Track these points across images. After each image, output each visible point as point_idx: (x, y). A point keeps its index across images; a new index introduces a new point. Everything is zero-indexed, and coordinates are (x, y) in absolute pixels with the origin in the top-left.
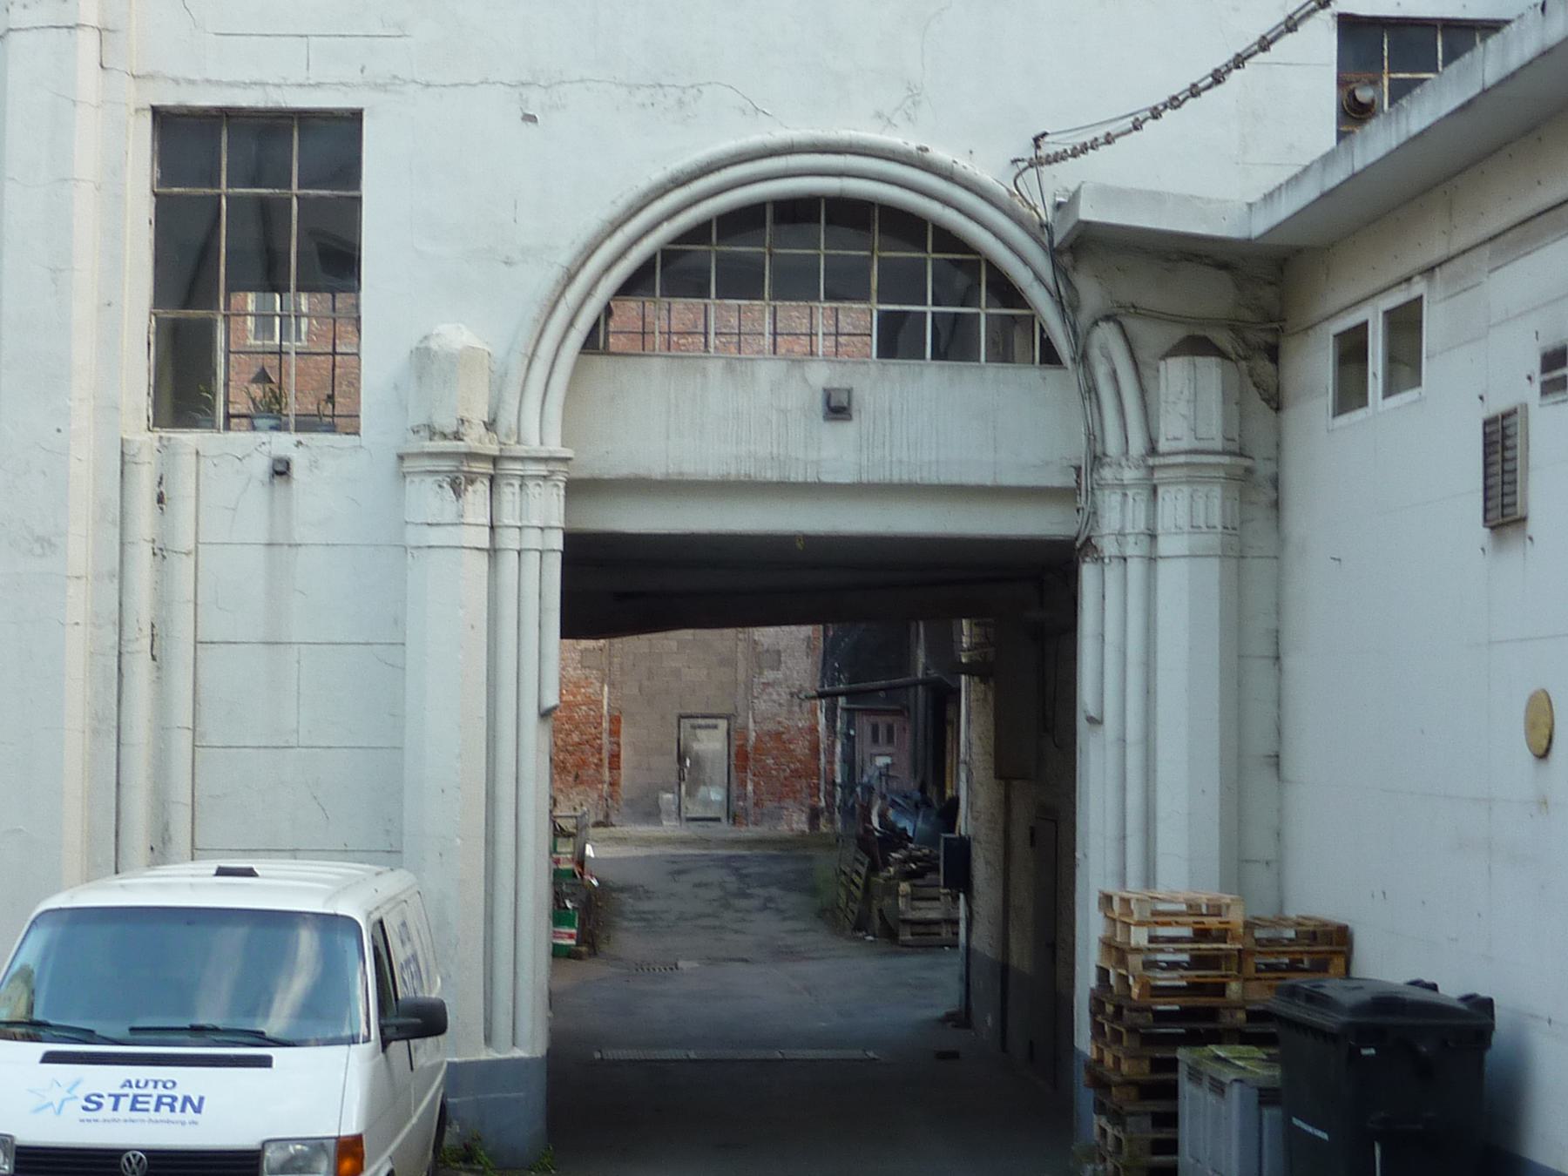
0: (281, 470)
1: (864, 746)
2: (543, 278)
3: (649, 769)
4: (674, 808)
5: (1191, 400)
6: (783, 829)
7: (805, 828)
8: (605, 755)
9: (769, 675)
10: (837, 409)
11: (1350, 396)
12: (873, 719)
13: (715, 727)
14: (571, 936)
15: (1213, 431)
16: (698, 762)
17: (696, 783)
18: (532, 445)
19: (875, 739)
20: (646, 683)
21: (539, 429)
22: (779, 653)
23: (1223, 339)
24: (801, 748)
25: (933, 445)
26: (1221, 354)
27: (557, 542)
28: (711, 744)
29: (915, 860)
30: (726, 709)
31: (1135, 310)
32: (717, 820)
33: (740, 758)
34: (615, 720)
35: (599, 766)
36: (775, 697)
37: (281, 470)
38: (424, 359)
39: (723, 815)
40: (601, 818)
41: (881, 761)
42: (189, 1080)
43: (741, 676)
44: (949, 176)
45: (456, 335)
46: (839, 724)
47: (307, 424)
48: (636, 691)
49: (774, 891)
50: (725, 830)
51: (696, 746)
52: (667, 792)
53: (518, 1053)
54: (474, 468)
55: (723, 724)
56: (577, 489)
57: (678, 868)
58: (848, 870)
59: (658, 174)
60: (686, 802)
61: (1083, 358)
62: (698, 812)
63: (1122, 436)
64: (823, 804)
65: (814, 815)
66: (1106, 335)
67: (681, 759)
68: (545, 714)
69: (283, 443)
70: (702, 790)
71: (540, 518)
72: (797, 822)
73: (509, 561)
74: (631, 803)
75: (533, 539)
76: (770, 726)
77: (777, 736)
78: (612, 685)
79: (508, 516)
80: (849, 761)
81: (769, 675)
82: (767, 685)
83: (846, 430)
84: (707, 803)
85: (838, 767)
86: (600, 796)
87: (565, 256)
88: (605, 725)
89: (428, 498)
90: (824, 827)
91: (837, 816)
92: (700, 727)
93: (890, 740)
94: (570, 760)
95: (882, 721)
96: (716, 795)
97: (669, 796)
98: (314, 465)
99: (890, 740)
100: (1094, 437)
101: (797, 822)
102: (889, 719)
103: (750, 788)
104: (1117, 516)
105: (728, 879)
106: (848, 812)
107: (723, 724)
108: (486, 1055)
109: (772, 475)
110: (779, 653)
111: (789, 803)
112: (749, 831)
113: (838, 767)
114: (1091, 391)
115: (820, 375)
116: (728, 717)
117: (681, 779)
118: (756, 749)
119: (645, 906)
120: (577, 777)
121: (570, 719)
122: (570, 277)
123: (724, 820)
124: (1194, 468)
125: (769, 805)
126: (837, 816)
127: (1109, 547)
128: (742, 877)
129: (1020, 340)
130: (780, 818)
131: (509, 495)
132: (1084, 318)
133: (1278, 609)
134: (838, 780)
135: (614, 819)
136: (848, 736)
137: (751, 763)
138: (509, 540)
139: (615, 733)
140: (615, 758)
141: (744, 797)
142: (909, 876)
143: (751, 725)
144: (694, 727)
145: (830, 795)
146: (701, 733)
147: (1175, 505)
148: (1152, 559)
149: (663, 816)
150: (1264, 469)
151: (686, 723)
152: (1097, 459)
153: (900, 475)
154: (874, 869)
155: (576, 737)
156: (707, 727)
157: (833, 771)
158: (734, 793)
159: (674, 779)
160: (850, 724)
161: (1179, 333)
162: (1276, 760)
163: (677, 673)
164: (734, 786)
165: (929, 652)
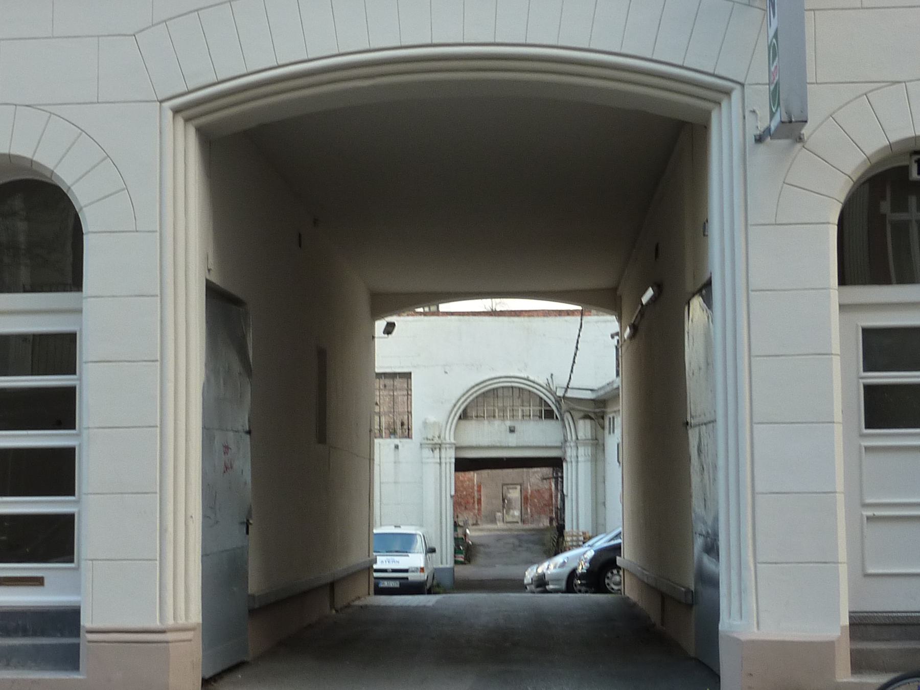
0: (397, 447)
2: (449, 406)
5: (584, 428)
6: (541, 525)
10: (512, 430)
11: (610, 433)
15: (589, 436)
16: (509, 501)
18: (448, 441)
21: (449, 438)
23: (593, 416)
24: (547, 496)
25: (536, 436)
26: (591, 418)
27: (453, 460)
30: (521, 481)
31: (573, 409)
33: (525, 499)
34: (479, 487)
37: (397, 447)
38: (425, 424)
42: (396, 558)
44: (534, 382)
45: (432, 419)
47: (403, 437)
49: (530, 545)
50: (520, 525)
51: (509, 495)
53: (448, 566)
54: (437, 447)
55: (519, 487)
56: (458, 448)
57: (499, 539)
59: (473, 384)
61: (563, 420)
62: (509, 519)
63: (571, 436)
65: (551, 520)
66: (567, 415)
67: (503, 500)
68: (451, 497)
69: (397, 441)
70: (511, 512)
71: (450, 456)
72: (546, 523)
73: (443, 465)
75: (448, 460)
76: (535, 488)
79: (443, 456)
83: (514, 435)
84: (513, 516)
87: (454, 402)
88: (476, 488)
89: (427, 453)
96: (517, 513)
98: (403, 446)
100: (565, 436)
104: (570, 453)
108: (441, 566)
109: (498, 444)
112: (527, 526)
114: (564, 426)
115: (508, 423)
117: (503, 507)
119: (487, 550)
122: (455, 405)
124: (585, 445)
125: (536, 516)
127: (568, 459)
128: (520, 541)
129: (549, 415)
131: (443, 451)
132: (562, 411)
133: (604, 471)
138: (443, 461)
139: (479, 491)
145: (556, 513)
146: (511, 491)
147: (581, 450)
148: (577, 462)
150: (601, 442)
151: (505, 487)
152: (566, 441)
153: (525, 444)
161: (582, 414)
162: (604, 504)
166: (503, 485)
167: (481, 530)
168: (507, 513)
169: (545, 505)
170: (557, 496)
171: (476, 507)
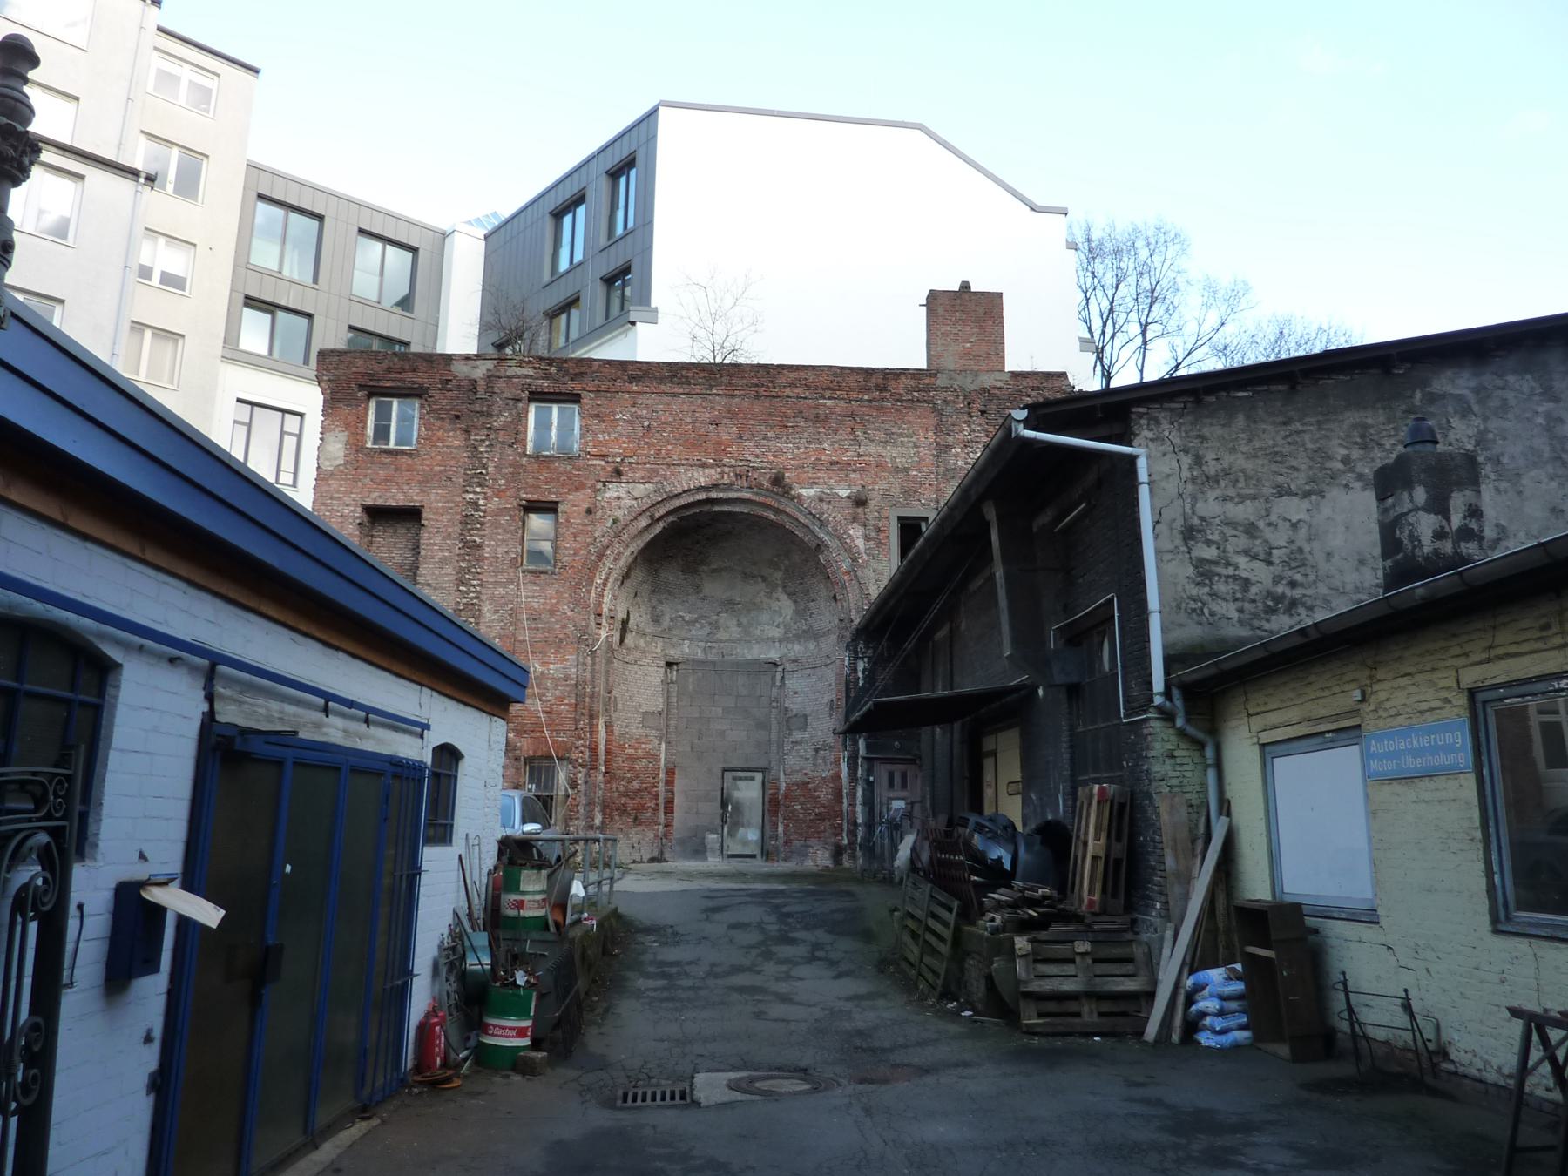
1: (881, 791)
4: (717, 846)
6: (809, 865)
7: (829, 863)
8: (661, 801)
9: (797, 735)
12: (890, 767)
13: (753, 779)
14: (521, 1033)
16: (738, 808)
17: (736, 825)
19: (891, 785)
22: (805, 716)
24: (825, 794)
28: (749, 792)
29: (1032, 903)
30: (762, 764)
32: (753, 856)
33: (773, 804)
34: (670, 772)
35: (655, 810)
39: (757, 851)
40: (655, 854)
41: (898, 804)
43: (774, 736)
49: (821, 935)
50: (760, 865)
51: (737, 794)
55: (759, 776)
57: (714, 905)
58: (918, 913)
60: (728, 841)
62: (736, 849)
64: (845, 842)
65: (838, 853)
67: (724, 805)
70: (741, 831)
74: (682, 842)
76: (797, 777)
78: (668, 743)
80: (869, 802)
81: (797, 735)
84: (745, 843)
85: (859, 809)
86: (656, 836)
88: (662, 776)
90: (846, 863)
91: (859, 853)
94: (631, 804)
95: (898, 769)
96: (753, 835)
99: (904, 786)
101: (820, 858)
103: (780, 829)
105: (767, 919)
106: (869, 849)
107: (759, 776)
110: (805, 716)
111: (813, 842)
112: (781, 867)
113: (859, 809)
116: (763, 770)
117: (724, 822)
118: (786, 797)
119: (672, 954)
120: (636, 818)
121: (631, 769)
126: (859, 853)
128: (784, 917)
130: (806, 855)
135: (667, 856)
136: (870, 784)
137: (782, 809)
139: (669, 782)
140: (669, 805)
141: (775, 837)
142: (1025, 926)
143: (782, 777)
144: (735, 778)
145: (852, 834)
146: (741, 784)
151: (728, 775)
154: (970, 912)
155: (636, 785)
156: (746, 778)
157: (854, 813)
158: (767, 835)
159: (718, 821)
160: (869, 771)
163: (722, 733)
164: (767, 827)
165: (1016, 641)
167: (667, 874)
168: (731, 834)
169: (821, 817)
170: (853, 794)
171: (661, 817)
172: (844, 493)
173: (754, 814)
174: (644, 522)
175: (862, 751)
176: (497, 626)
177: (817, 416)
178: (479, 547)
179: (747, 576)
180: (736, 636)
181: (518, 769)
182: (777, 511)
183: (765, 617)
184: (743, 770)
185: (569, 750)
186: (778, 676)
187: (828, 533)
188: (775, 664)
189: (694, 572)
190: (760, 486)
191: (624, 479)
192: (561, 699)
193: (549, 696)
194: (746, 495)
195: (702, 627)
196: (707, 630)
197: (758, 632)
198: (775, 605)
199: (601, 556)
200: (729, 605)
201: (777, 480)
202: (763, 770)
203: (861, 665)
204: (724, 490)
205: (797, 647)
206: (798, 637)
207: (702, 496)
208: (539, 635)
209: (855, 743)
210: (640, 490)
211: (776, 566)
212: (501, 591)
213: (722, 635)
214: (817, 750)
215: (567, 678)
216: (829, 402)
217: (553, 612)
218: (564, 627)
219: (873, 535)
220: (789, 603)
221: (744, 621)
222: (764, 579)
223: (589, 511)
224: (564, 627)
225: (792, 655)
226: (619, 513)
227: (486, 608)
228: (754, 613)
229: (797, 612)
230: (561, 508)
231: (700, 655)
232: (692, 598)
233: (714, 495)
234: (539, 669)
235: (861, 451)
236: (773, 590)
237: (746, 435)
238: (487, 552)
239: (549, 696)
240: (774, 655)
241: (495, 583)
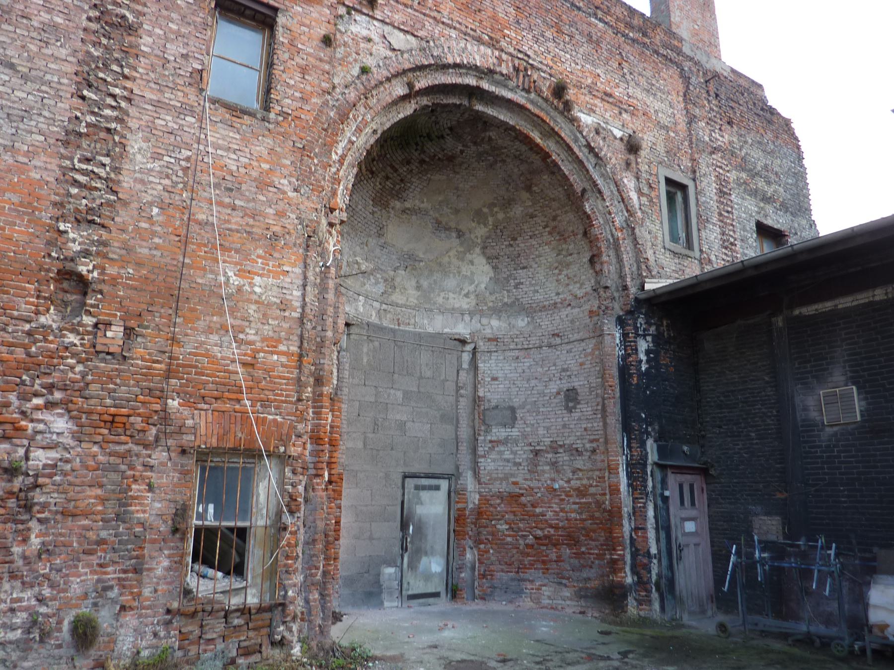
3: (371, 538)
4: (395, 584)
9: (498, 433)
12: (681, 478)
13: (437, 488)
17: (419, 553)
20: (370, 435)
22: (513, 410)
28: (433, 507)
30: (448, 468)
32: (436, 595)
33: (461, 523)
36: (507, 455)
39: (441, 589)
43: (465, 432)
46: (650, 484)
48: (360, 445)
51: (420, 510)
52: (390, 565)
55: (444, 484)
60: (409, 577)
62: (417, 586)
67: (404, 526)
70: (424, 560)
74: (350, 582)
77: (513, 498)
81: (498, 433)
82: (495, 443)
92: (424, 488)
93: (693, 503)
95: (687, 479)
96: (436, 565)
97: (391, 570)
99: (693, 503)
102: (689, 477)
107: (444, 484)
110: (513, 410)
111: (531, 574)
113: (651, 534)
116: (448, 477)
117: (404, 549)
123: (443, 595)
125: (503, 577)
130: (519, 593)
134: (654, 550)
144: (417, 488)
146: (425, 495)
149: (385, 596)
151: (410, 483)
159: (397, 549)
163: (402, 425)
166: (405, 477)
168: (412, 566)
170: (638, 513)
172: (618, 134)
173: (438, 536)
174: (400, 90)
175: (652, 456)
176: (157, 187)
177: (589, 35)
178: (131, 29)
179: (440, 226)
180: (413, 301)
181: (185, 473)
182: (552, 134)
183: (451, 282)
184: (427, 476)
185: (285, 441)
186: (466, 357)
187: (602, 175)
188: (463, 342)
189: (385, 206)
190: (539, 93)
191: (378, 14)
192: (272, 343)
193: (251, 334)
194: (519, 97)
195: (377, 283)
196: (381, 288)
197: (440, 300)
198: (466, 270)
199: (343, 118)
200: (410, 261)
201: (559, 90)
202: (448, 477)
203: (643, 345)
204: (497, 83)
205: (495, 323)
206: (496, 311)
207: (472, 81)
208: (236, 220)
209: (643, 444)
210: (399, 40)
211: (479, 217)
212: (167, 120)
213: (397, 297)
214: (537, 453)
215: (284, 306)
216: (601, 25)
217: (263, 184)
218: (281, 214)
219: (646, 190)
220: (487, 268)
221: (425, 284)
222: (460, 234)
223: (327, 41)
224: (281, 214)
225: (488, 332)
226: (370, 62)
227: (136, 144)
228: (437, 276)
229: (495, 280)
230: (281, 20)
231: (374, 319)
232: (373, 242)
233: (485, 85)
234: (235, 281)
235: (630, 91)
236: (469, 250)
237: (524, 23)
238: (145, 43)
239: (251, 334)
240: (462, 329)
241: (158, 105)
